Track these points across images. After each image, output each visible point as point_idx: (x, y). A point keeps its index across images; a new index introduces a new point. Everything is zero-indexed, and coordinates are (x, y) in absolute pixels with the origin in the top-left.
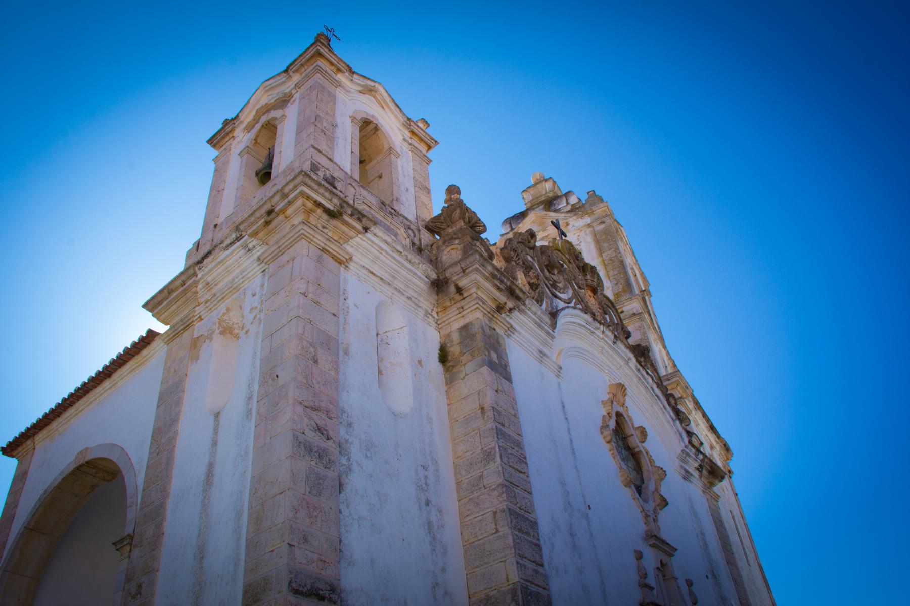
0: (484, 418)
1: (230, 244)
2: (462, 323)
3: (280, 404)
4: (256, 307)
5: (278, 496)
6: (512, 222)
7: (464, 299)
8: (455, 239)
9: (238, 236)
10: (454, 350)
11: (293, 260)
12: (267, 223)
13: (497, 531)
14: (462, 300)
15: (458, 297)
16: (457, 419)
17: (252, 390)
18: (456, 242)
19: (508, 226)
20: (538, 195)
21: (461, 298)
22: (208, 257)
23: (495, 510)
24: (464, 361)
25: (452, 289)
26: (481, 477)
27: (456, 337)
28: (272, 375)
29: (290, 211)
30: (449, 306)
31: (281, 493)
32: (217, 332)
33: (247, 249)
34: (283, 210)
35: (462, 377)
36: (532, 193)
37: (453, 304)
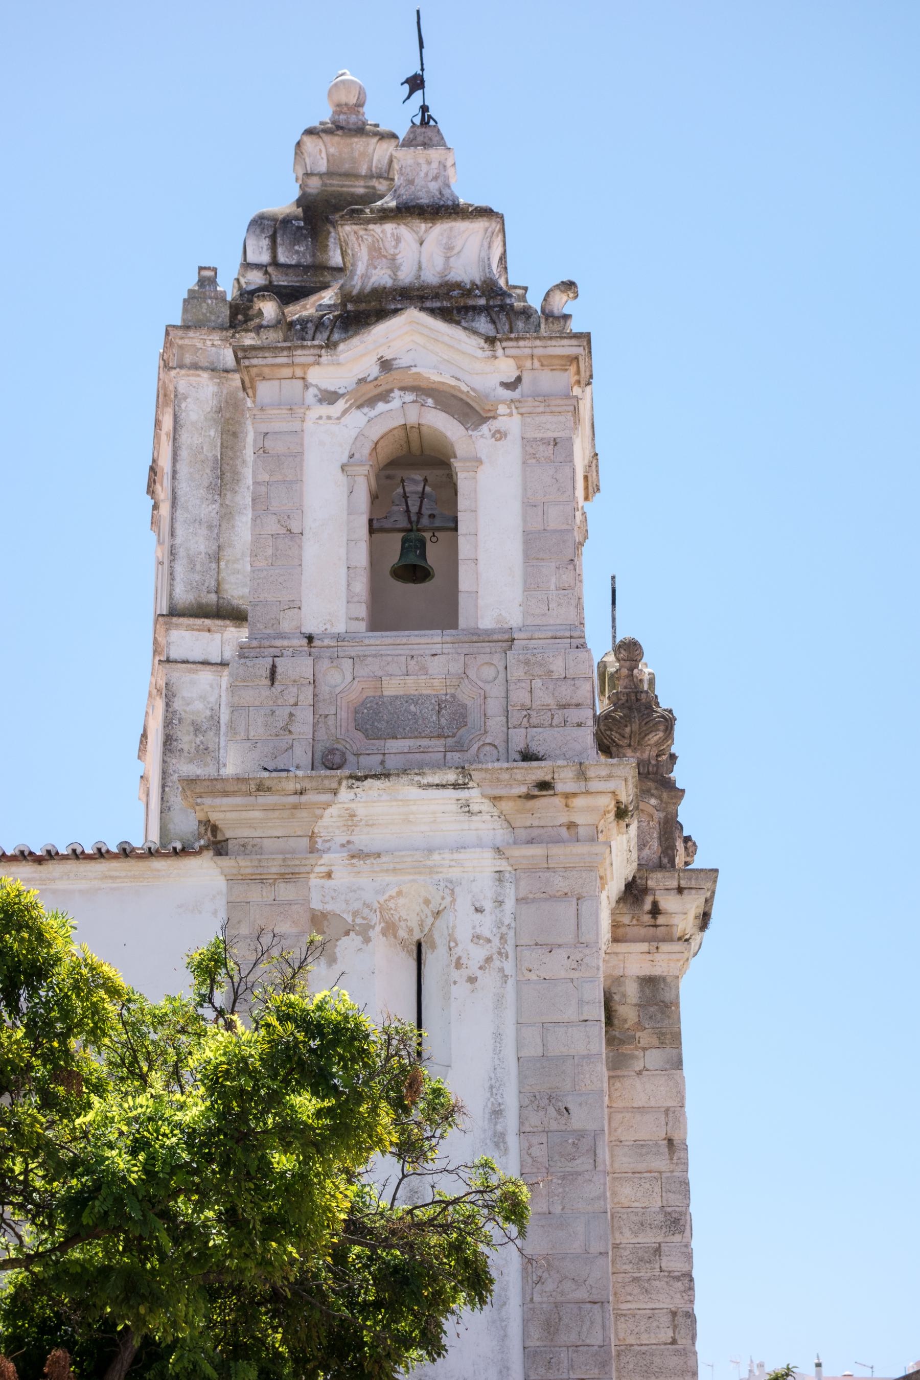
0: (671, 1159)
1: (437, 785)
2: (647, 970)
3: (578, 1162)
4: (489, 941)
5: (589, 1306)
6: (279, 240)
7: (656, 926)
8: (652, 795)
9: (460, 782)
10: (627, 1012)
11: (578, 899)
12: (529, 797)
13: (674, 1342)
14: (653, 926)
15: (647, 918)
16: (622, 1139)
17: (500, 1101)
18: (653, 801)
19: (265, 243)
20: (347, 167)
21: (652, 922)
22: (379, 779)
23: (673, 1309)
24: (643, 1043)
25: (648, 906)
26: (658, 1251)
27: (632, 990)
28: (553, 1101)
29: (578, 802)
30: (624, 925)
31: (595, 1303)
32: (378, 928)
33: (467, 809)
34: (567, 796)
35: (637, 1069)
36: (332, 150)
37: (633, 926)
